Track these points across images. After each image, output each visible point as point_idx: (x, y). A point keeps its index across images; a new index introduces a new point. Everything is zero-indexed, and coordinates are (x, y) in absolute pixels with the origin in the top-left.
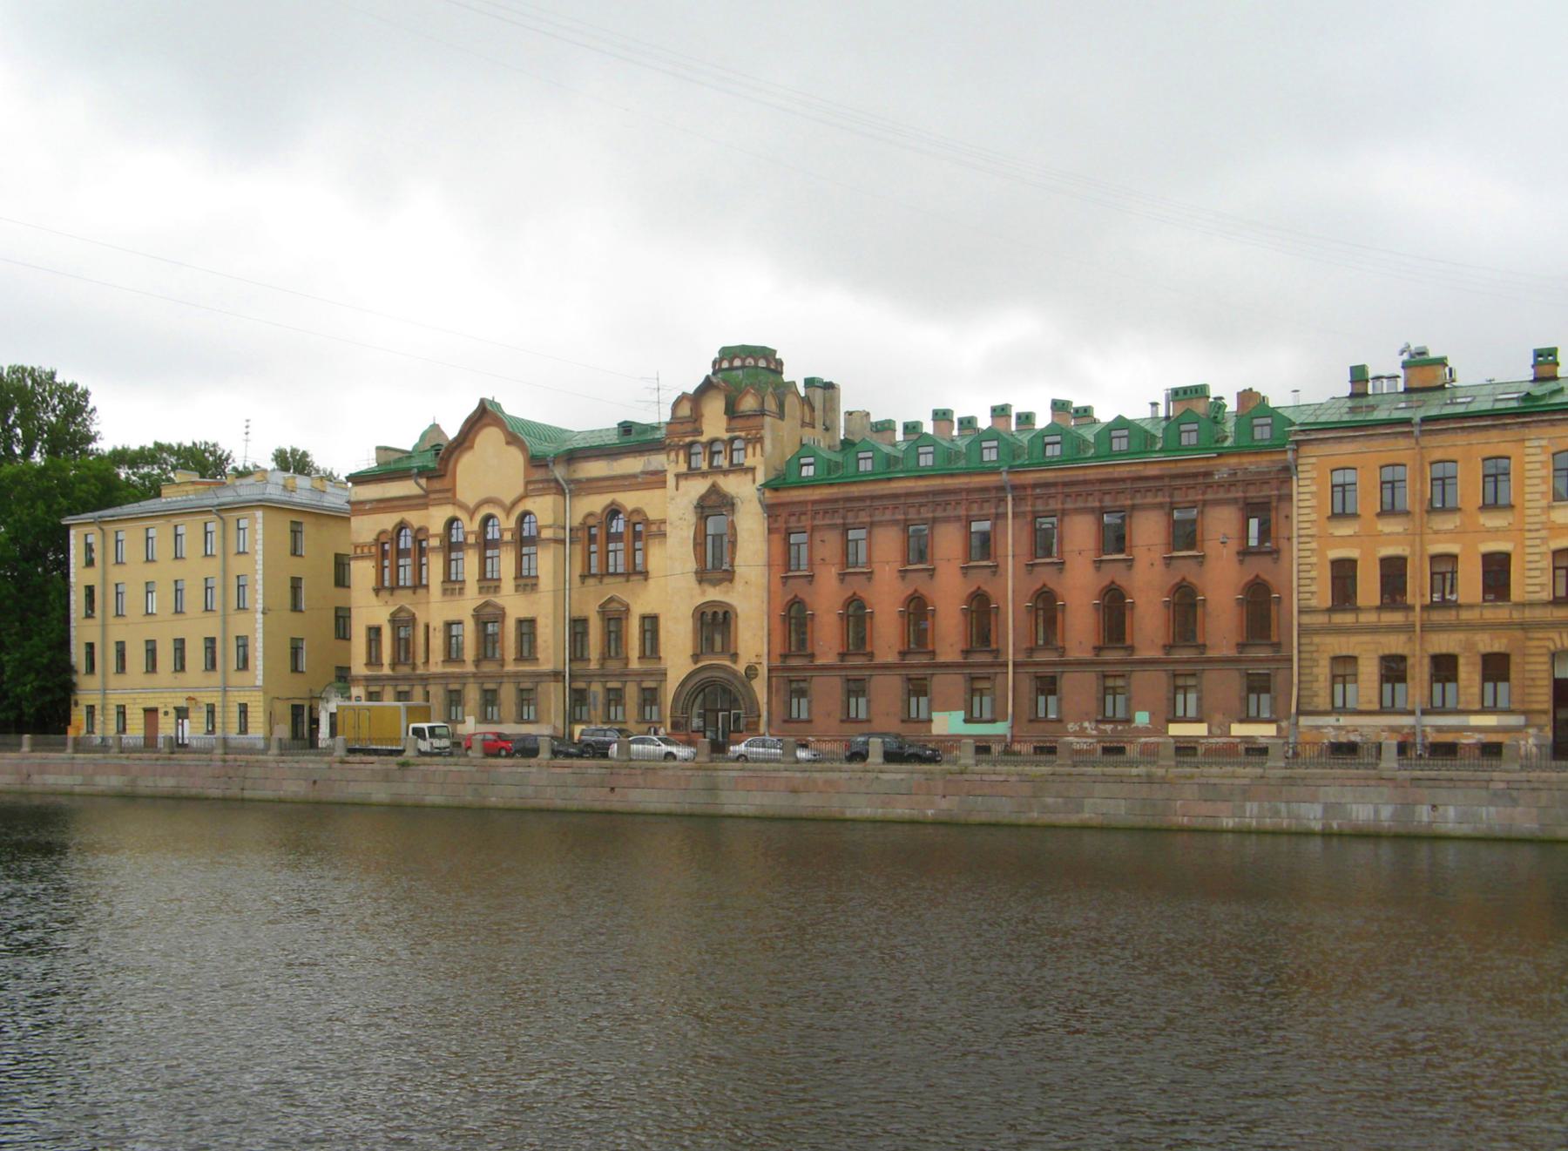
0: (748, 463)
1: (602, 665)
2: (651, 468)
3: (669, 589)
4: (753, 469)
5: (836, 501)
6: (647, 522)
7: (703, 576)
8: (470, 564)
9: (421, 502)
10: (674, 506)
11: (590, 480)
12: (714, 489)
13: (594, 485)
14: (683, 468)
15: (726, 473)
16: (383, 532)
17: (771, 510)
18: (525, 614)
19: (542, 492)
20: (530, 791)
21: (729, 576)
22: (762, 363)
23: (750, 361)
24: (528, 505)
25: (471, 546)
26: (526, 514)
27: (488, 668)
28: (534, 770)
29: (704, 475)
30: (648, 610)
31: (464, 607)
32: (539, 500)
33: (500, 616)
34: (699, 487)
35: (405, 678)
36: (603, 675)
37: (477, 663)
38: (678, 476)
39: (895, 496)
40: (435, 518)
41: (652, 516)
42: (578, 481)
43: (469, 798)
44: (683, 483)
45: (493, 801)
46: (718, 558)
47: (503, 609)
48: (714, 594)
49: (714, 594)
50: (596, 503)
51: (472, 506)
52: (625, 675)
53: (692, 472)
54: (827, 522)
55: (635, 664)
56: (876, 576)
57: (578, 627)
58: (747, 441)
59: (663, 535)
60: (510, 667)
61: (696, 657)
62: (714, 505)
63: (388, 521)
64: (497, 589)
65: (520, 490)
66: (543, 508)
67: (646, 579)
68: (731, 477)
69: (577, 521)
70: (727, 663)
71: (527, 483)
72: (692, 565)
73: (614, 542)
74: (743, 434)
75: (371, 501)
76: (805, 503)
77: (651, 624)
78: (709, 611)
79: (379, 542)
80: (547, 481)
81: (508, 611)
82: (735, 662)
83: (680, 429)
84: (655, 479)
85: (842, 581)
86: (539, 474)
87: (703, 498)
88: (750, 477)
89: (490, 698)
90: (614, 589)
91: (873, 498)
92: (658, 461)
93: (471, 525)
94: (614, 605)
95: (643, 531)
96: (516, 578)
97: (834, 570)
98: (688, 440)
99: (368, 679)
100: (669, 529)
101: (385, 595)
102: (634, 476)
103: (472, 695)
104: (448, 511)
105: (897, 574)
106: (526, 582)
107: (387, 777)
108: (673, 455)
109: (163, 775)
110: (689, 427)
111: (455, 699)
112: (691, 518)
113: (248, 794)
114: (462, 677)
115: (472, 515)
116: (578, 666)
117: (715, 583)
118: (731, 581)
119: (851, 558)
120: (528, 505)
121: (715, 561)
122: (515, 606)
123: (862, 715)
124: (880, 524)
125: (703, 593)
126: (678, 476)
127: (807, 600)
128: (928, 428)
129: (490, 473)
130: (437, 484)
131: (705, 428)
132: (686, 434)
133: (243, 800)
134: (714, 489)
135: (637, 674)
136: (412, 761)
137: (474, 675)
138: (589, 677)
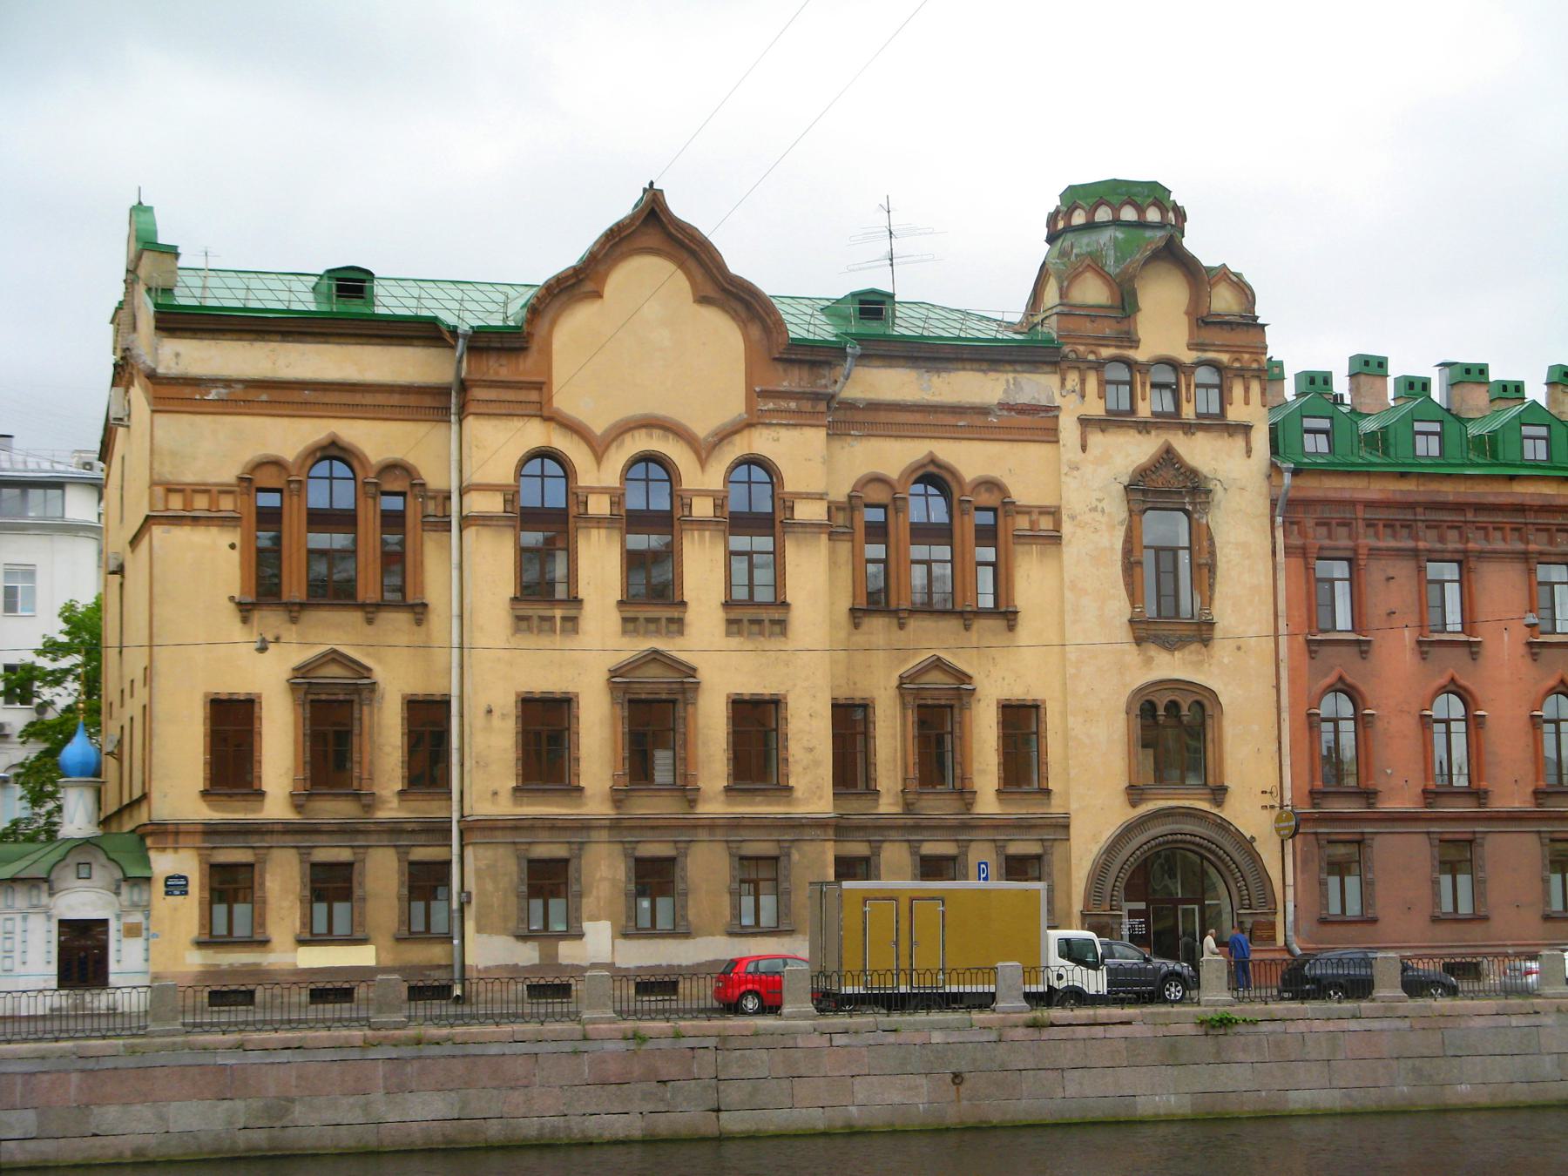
0: (1235, 413)
1: (908, 807)
2: (1024, 398)
3: (1066, 645)
4: (1246, 429)
5: (1411, 506)
6: (1005, 507)
7: (1145, 632)
8: (599, 564)
9: (436, 404)
10: (1082, 478)
11: (875, 406)
12: (1168, 457)
13: (883, 417)
14: (1096, 408)
15: (1188, 428)
16: (277, 463)
17: (1289, 511)
18: (750, 686)
19: (798, 420)
20: (1548, 1065)
21: (1202, 632)
22: (1153, 215)
23: (1128, 214)
24: (761, 442)
25: (599, 521)
26: (752, 461)
27: (646, 807)
28: (1548, 1020)
29: (1144, 427)
30: (1018, 691)
31: (587, 660)
32: (786, 435)
33: (686, 681)
34: (1132, 451)
35: (345, 831)
36: (911, 826)
37: (618, 797)
38: (1085, 422)
39: (1521, 509)
40: (494, 448)
41: (1022, 494)
42: (850, 406)
43: (1402, 1090)
44: (1096, 439)
45: (1463, 1091)
46: (1167, 594)
47: (692, 671)
48: (1170, 666)
49: (1170, 666)
50: (895, 456)
51: (598, 427)
52: (967, 827)
53: (1118, 420)
54: (1392, 543)
55: (988, 803)
56: (1489, 650)
57: (850, 721)
58: (1242, 373)
59: (1055, 539)
60: (714, 805)
61: (1135, 793)
62: (1167, 488)
63: (289, 437)
64: (677, 625)
65: (735, 407)
66: (810, 463)
67: (1011, 628)
68: (1200, 436)
69: (840, 493)
70: (1204, 806)
71: (757, 394)
72: (1119, 607)
73: (939, 548)
74: (1225, 358)
75: (228, 383)
76: (1353, 503)
77: (1021, 721)
78: (1162, 701)
79: (247, 483)
80: (816, 397)
81: (706, 675)
82: (1219, 803)
83: (1088, 328)
84: (1036, 423)
85: (1423, 656)
86: (791, 380)
87: (1143, 473)
88: (1239, 442)
89: (654, 878)
90: (932, 640)
91: (1480, 508)
92: (1037, 386)
93: (599, 476)
94: (936, 678)
95: (1002, 524)
96: (728, 605)
97: (1409, 636)
98: (1106, 352)
99: (211, 831)
100: (1067, 528)
101: (270, 621)
102: (983, 411)
103: (604, 871)
104: (535, 434)
105: (1522, 649)
106: (757, 613)
107: (1172, 1053)
108: (1073, 379)
109: (396, 1088)
110: (1108, 328)
111: (548, 880)
112: (1118, 510)
113: (732, 1122)
114: (585, 826)
115: (599, 448)
116: (854, 807)
117: (1170, 644)
118: (1206, 641)
119: (1434, 617)
120: (761, 442)
121: (1168, 605)
122: (723, 668)
123: (1465, 908)
124: (1482, 555)
125: (1149, 661)
126: (1085, 422)
127: (1362, 688)
128: (1341, 385)
129: (648, 366)
130: (500, 368)
131: (1142, 332)
132: (1103, 341)
133: (722, 1139)
134: (1168, 457)
135: (995, 824)
136: (1237, 1011)
137: (615, 825)
138: (879, 830)
